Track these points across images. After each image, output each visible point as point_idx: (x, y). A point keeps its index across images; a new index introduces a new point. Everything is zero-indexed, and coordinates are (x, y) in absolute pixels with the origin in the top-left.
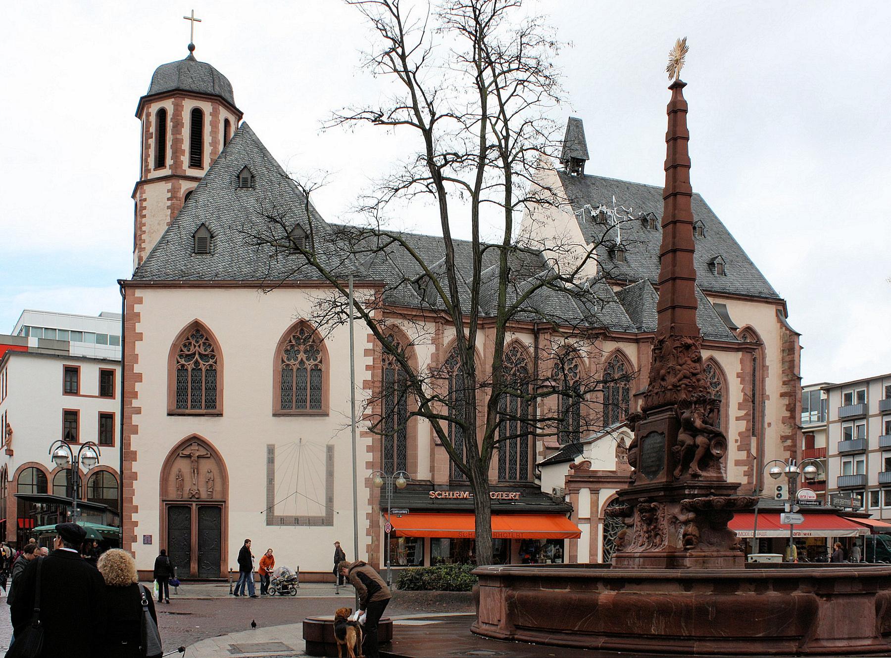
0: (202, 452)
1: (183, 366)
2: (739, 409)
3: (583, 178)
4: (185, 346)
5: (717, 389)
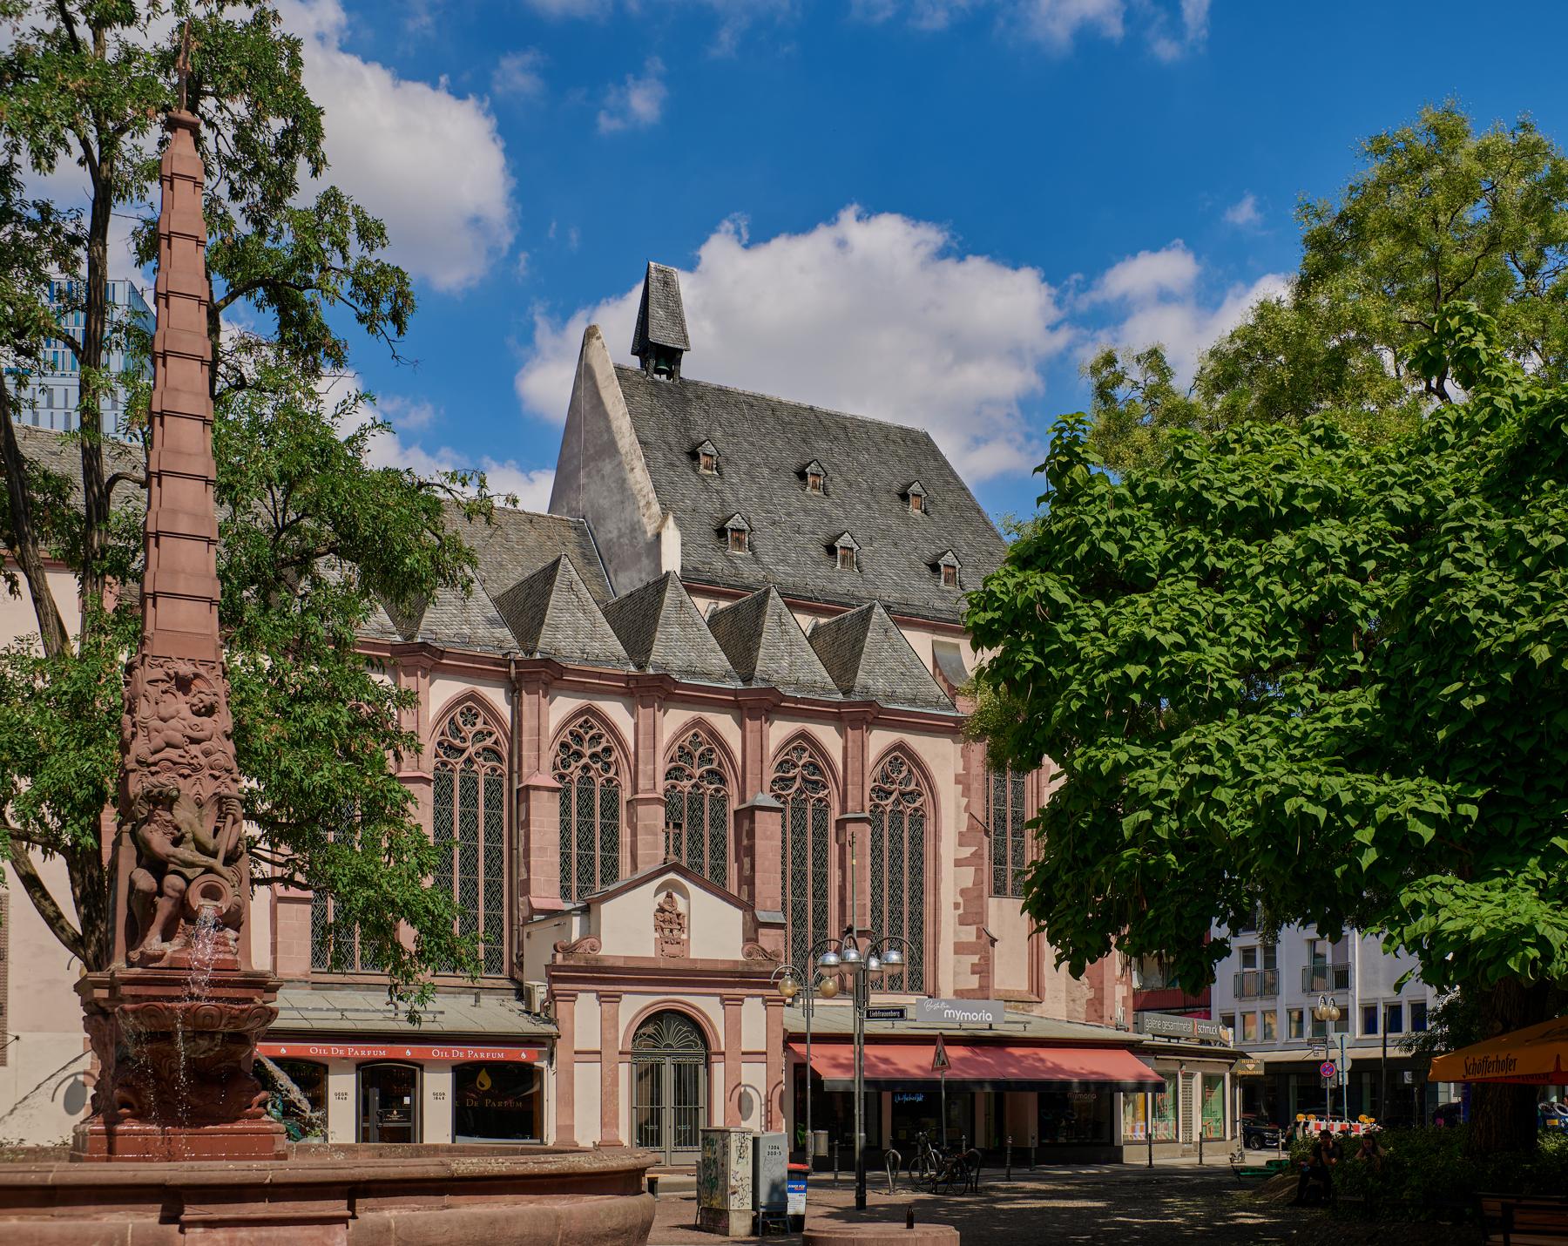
2: (961, 845)
3: (686, 395)
5: (917, 805)
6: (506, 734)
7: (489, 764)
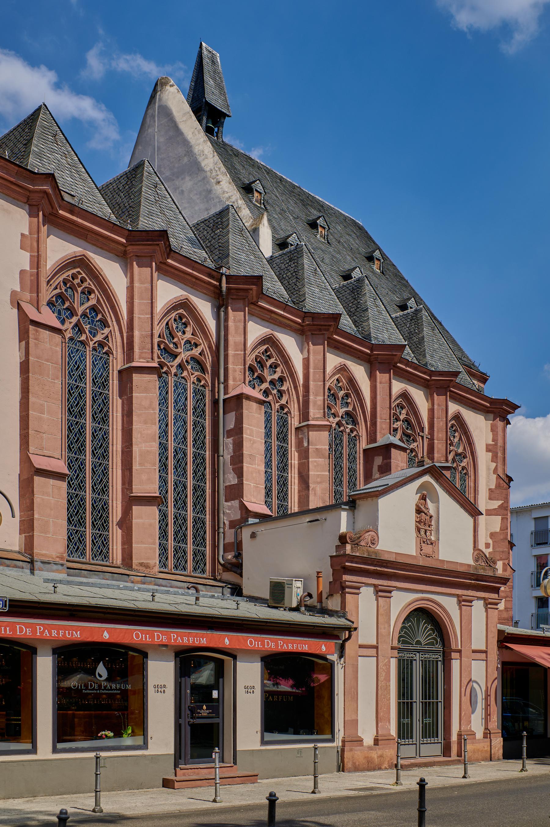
2: (490, 499)
6: (210, 347)
7: (197, 373)
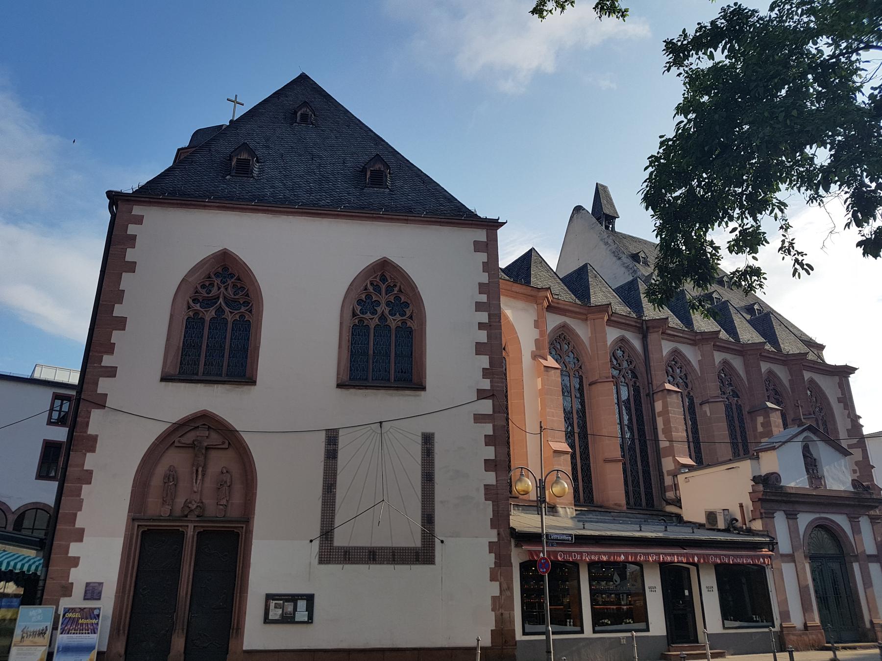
0: (215, 438)
1: (196, 313)
4: (203, 286)
